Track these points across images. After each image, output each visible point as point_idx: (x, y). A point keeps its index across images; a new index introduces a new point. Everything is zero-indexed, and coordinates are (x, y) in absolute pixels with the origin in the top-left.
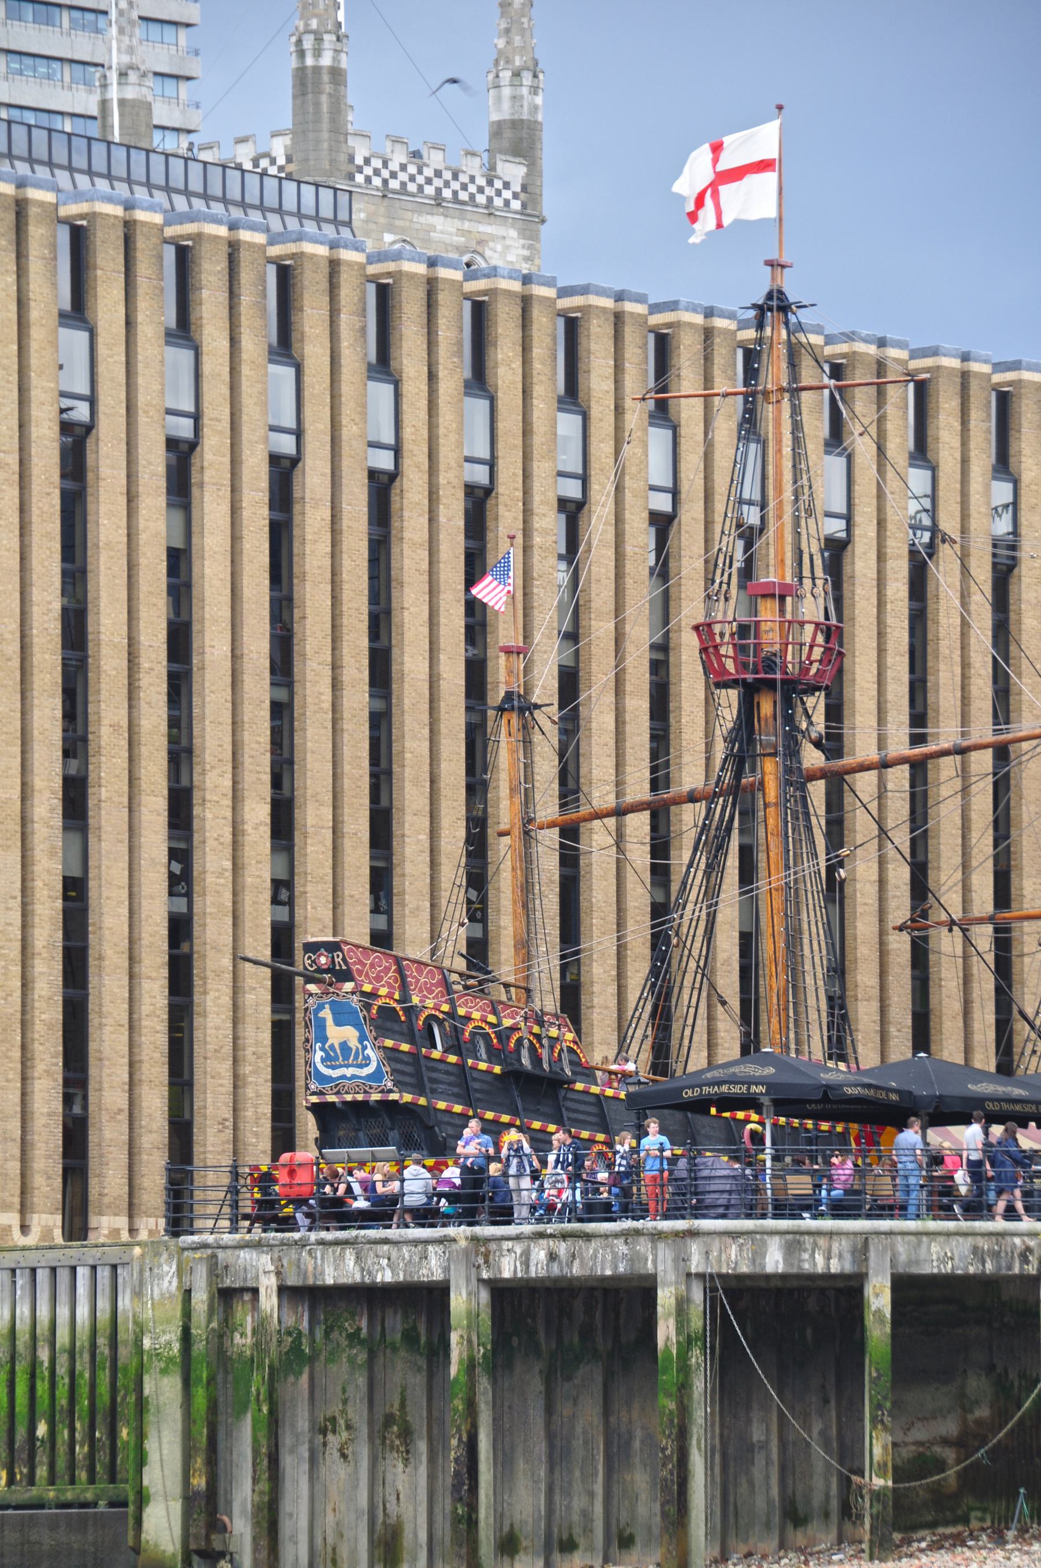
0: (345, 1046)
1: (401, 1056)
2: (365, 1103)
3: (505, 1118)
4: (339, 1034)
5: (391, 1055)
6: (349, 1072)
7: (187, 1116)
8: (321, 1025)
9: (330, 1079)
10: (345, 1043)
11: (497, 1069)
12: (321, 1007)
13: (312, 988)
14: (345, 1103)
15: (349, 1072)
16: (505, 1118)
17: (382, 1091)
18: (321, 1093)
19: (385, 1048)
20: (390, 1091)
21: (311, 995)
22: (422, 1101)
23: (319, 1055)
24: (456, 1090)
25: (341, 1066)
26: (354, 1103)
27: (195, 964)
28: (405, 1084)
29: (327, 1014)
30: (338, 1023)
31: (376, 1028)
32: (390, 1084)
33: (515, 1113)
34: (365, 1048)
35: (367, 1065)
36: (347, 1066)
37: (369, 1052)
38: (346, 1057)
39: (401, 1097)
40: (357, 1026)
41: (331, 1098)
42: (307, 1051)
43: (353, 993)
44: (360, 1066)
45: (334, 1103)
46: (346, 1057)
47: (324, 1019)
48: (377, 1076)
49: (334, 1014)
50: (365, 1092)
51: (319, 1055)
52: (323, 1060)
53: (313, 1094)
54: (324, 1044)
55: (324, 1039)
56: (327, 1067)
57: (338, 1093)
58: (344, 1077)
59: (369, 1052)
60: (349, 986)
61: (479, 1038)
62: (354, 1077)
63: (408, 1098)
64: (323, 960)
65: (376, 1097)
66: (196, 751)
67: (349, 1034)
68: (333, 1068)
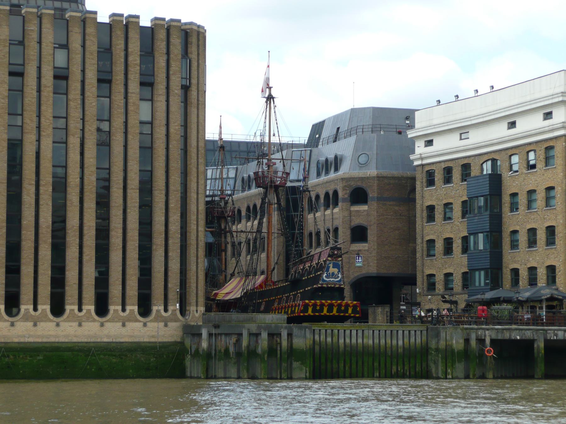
0: (333, 274)
6: (332, 280)
8: (328, 268)
9: (326, 281)
12: (330, 263)
13: (329, 259)
14: (328, 287)
15: (332, 280)
18: (322, 284)
23: (325, 275)
26: (331, 287)
29: (331, 265)
30: (333, 267)
37: (340, 275)
40: (339, 269)
41: (324, 286)
48: (340, 281)
51: (325, 275)
55: (328, 270)
57: (327, 285)
59: (340, 275)
60: (340, 259)
65: (337, 286)
67: (336, 270)
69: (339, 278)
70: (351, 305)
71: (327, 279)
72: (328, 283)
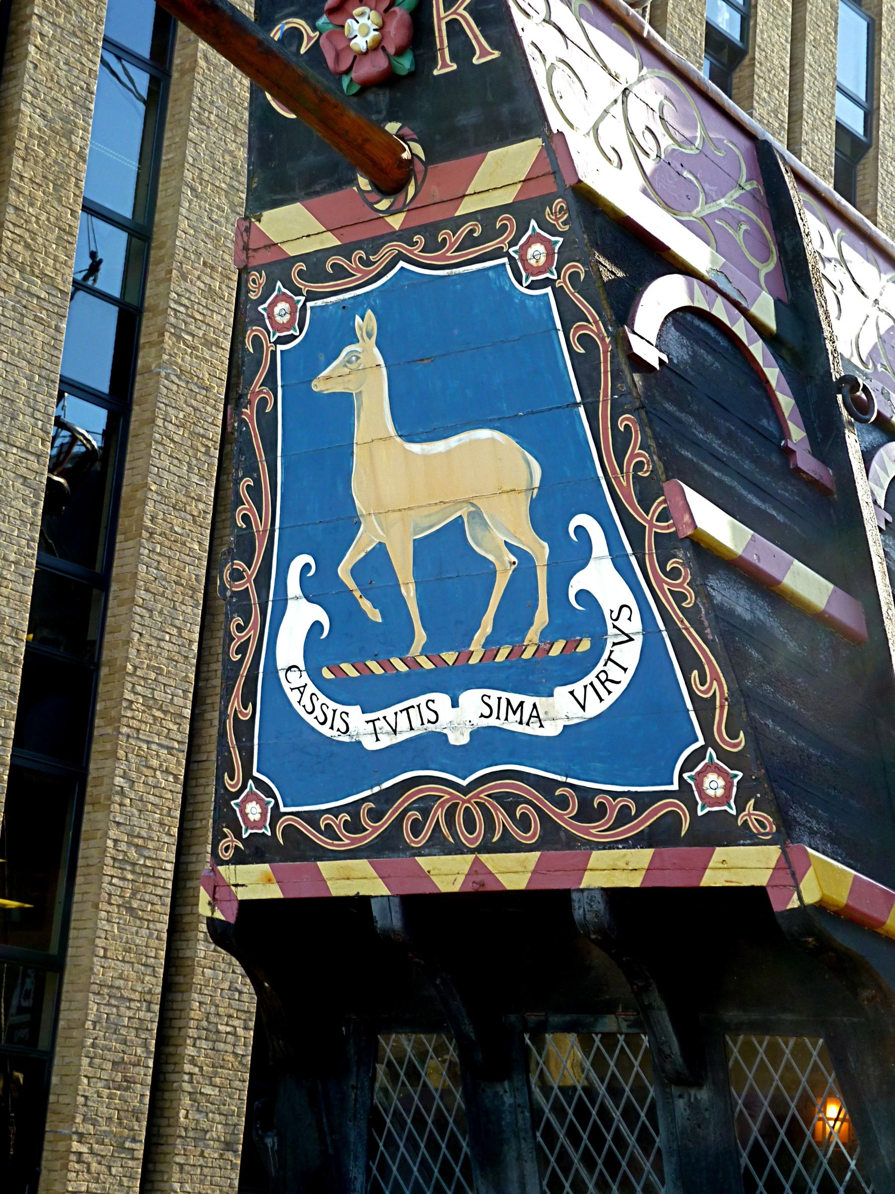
0: (447, 553)
2: (546, 906)
4: (434, 483)
6: (461, 716)
7: (43, 1045)
12: (331, 336)
13: (293, 227)
15: (461, 716)
18: (287, 848)
19: (705, 553)
20: (720, 832)
21: (280, 268)
27: (101, 688)
29: (361, 373)
30: (418, 419)
34: (572, 555)
36: (453, 681)
37: (601, 580)
38: (451, 627)
39: (790, 870)
41: (350, 878)
43: (524, 210)
44: (536, 678)
45: (362, 902)
46: (451, 627)
47: (343, 406)
48: (639, 728)
50: (552, 838)
53: (255, 851)
54: (328, 561)
57: (386, 847)
58: (428, 746)
59: (601, 580)
62: (487, 741)
64: (362, 29)
65: (616, 868)
66: (158, 236)
68: (372, 696)
71: (360, 727)
72: (397, 801)
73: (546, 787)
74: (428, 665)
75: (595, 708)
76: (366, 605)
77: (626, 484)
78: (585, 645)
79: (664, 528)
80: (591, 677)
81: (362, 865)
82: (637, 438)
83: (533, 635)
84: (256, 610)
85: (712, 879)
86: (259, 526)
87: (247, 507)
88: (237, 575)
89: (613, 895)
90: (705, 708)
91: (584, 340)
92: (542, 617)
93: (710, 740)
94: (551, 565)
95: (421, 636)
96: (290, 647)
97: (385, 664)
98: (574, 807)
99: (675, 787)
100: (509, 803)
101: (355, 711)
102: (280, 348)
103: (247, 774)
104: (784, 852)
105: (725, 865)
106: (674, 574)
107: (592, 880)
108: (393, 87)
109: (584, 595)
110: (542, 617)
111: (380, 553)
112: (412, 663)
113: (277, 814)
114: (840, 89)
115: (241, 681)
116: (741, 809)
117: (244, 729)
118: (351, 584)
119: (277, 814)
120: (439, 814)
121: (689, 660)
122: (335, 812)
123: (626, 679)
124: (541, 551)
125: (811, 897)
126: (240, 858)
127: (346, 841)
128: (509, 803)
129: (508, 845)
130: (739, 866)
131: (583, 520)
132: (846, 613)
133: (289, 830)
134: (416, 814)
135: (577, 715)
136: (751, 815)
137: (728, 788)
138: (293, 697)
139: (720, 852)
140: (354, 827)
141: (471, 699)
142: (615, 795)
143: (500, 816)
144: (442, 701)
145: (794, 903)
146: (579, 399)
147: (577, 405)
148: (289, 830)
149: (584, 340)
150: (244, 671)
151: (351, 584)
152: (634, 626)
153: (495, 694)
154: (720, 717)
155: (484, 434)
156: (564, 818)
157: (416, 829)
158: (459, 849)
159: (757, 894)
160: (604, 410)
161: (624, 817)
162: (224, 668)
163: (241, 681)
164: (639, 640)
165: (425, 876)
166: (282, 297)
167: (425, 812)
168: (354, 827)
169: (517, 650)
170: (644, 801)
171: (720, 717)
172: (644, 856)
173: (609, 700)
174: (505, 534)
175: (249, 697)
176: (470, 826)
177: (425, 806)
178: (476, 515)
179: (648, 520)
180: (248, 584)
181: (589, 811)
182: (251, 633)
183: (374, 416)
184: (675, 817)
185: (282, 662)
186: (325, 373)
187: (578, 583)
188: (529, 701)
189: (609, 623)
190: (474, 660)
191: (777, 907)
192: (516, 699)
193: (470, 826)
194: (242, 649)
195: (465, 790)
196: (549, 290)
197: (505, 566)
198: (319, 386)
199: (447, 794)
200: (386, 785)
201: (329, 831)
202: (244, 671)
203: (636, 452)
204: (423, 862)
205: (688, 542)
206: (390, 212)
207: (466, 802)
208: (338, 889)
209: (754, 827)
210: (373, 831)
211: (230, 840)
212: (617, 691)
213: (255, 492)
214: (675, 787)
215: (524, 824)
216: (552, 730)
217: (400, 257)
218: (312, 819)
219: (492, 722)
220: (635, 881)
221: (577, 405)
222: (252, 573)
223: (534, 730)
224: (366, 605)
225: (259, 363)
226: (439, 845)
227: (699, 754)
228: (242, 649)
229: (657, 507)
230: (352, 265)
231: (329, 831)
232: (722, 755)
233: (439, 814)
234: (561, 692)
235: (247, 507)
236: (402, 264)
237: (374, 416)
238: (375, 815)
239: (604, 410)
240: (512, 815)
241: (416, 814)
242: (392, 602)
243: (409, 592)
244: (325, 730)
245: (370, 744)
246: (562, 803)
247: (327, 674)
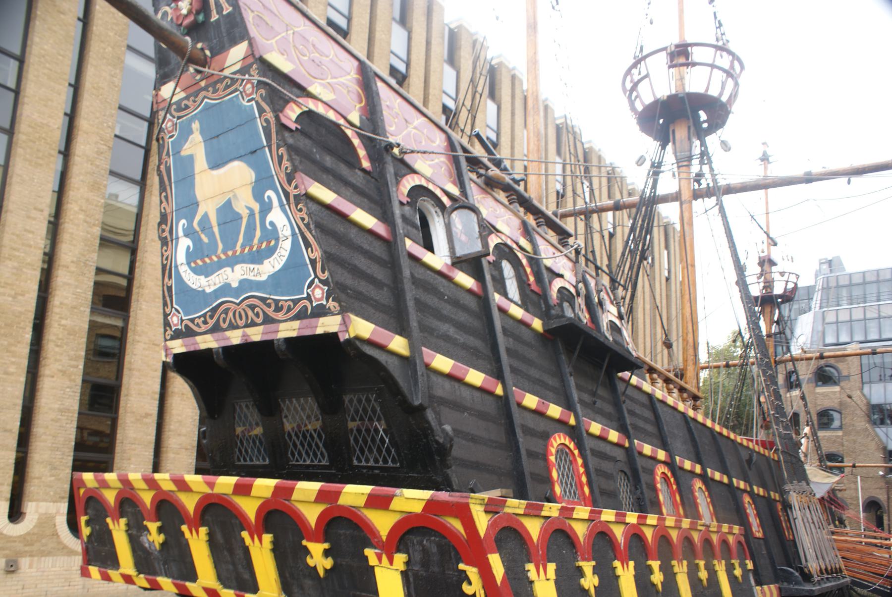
0: (227, 212)
1: (353, 233)
2: (266, 346)
3: (555, 411)
5: (326, 224)
6: (234, 275)
9: (201, 296)
10: (228, 204)
11: (537, 324)
14: (229, 351)
15: (234, 275)
16: (555, 411)
17: (301, 315)
20: (321, 312)
22: (398, 344)
24: (473, 341)
25: (220, 265)
26: (247, 347)
28: (359, 296)
31: (291, 148)
32: (319, 293)
33: (568, 406)
34: (266, 208)
35: (271, 251)
36: (232, 262)
38: (229, 241)
39: (345, 323)
40: (251, 155)
41: (207, 342)
42: (164, 242)
44: (258, 257)
45: (209, 350)
46: (229, 241)
49: (210, 139)
50: (268, 320)
52: (191, 257)
54: (190, 221)
56: (197, 271)
59: (277, 217)
61: (507, 269)
62: (245, 284)
63: (363, 328)
65: (288, 330)
69: (285, 247)
70: (383, 523)
73: (263, 300)
74: (223, 257)
75: (278, 267)
76: (203, 236)
77: (283, 176)
78: (273, 243)
79: (296, 192)
80: (275, 255)
81: (208, 337)
82: (285, 157)
83: (256, 241)
84: (170, 243)
85: (319, 331)
86: (168, 211)
87: (164, 204)
88: (163, 231)
89: (288, 340)
90: (313, 262)
91: (267, 121)
92: (258, 233)
93: (316, 276)
94: (261, 212)
95: (221, 246)
96: (181, 257)
97: (211, 259)
98: (273, 307)
99: (305, 295)
100: (252, 307)
101: (202, 277)
102: (171, 140)
103: (172, 307)
104: (343, 319)
105: (323, 325)
106: (301, 210)
107: (282, 335)
108: (195, 29)
109: (272, 223)
110: (258, 233)
111: (206, 216)
112: (219, 257)
113: (182, 321)
114: (488, 126)
115: (167, 271)
116: (327, 301)
117: (170, 289)
118: (198, 229)
119: (182, 321)
120: (231, 314)
121: (308, 245)
122: (199, 317)
123: (287, 254)
124: (256, 207)
125: (352, 335)
126: (173, 338)
127: (204, 328)
128: (252, 307)
129: (253, 324)
130: (328, 325)
131: (270, 193)
132: (381, 229)
133: (186, 326)
134: (223, 315)
135: (272, 271)
136: (332, 304)
137: (323, 294)
138: (183, 275)
139: (322, 320)
140: (205, 322)
141: (238, 268)
142: (286, 301)
143: (250, 313)
144: (228, 269)
145: (347, 337)
146: (265, 144)
147: (264, 147)
148: (186, 326)
149: (267, 121)
150: (168, 267)
151: (198, 229)
152: (288, 232)
153: (245, 265)
154: (319, 266)
155: (236, 164)
156: (270, 312)
157: (224, 321)
158: (237, 327)
159: (335, 335)
160: (274, 147)
161: (289, 309)
162: (167, 269)
163: (167, 271)
164: (290, 239)
165: (228, 339)
166: (170, 120)
167: (227, 314)
168: (205, 322)
169: (251, 247)
170: (296, 302)
171: (319, 266)
172: (296, 324)
173: (282, 263)
174: (245, 202)
175: (170, 277)
176: (241, 318)
177: (226, 311)
178: (235, 196)
179: (290, 189)
180: (166, 234)
181: (278, 309)
182: (169, 252)
183: (201, 163)
184: (306, 307)
185: (179, 263)
186: (185, 147)
187: (269, 218)
188: (256, 266)
189: (280, 233)
190: (238, 253)
191: (342, 340)
192: (252, 266)
193: (241, 318)
194: (167, 259)
195: (238, 304)
196: (253, 102)
197: (245, 213)
198: (183, 153)
199: (233, 306)
200: (214, 305)
201: (198, 325)
202: (168, 267)
203: (286, 163)
204: (228, 333)
205: (304, 197)
206: (202, 80)
207: (239, 309)
208: (203, 347)
209: (332, 308)
210: (211, 323)
211: (169, 332)
212: (284, 259)
213: (166, 197)
214: (305, 295)
215: (257, 315)
216: (264, 278)
217: (205, 97)
218: (192, 320)
219: (245, 277)
220: (294, 334)
221: (264, 147)
222: (168, 229)
223: (258, 278)
224: (203, 236)
225: (164, 147)
226: (233, 327)
227: (312, 282)
228: (167, 259)
229: (293, 184)
230: (190, 103)
231: (198, 325)
232: (320, 281)
233: (231, 314)
234: (266, 262)
235: (164, 204)
236: (206, 100)
237: (201, 163)
238: (212, 317)
239: (274, 147)
240: (253, 311)
241: (223, 315)
242: (211, 236)
243: (216, 230)
244: (194, 287)
245: (208, 290)
246: (269, 306)
247: (193, 265)
